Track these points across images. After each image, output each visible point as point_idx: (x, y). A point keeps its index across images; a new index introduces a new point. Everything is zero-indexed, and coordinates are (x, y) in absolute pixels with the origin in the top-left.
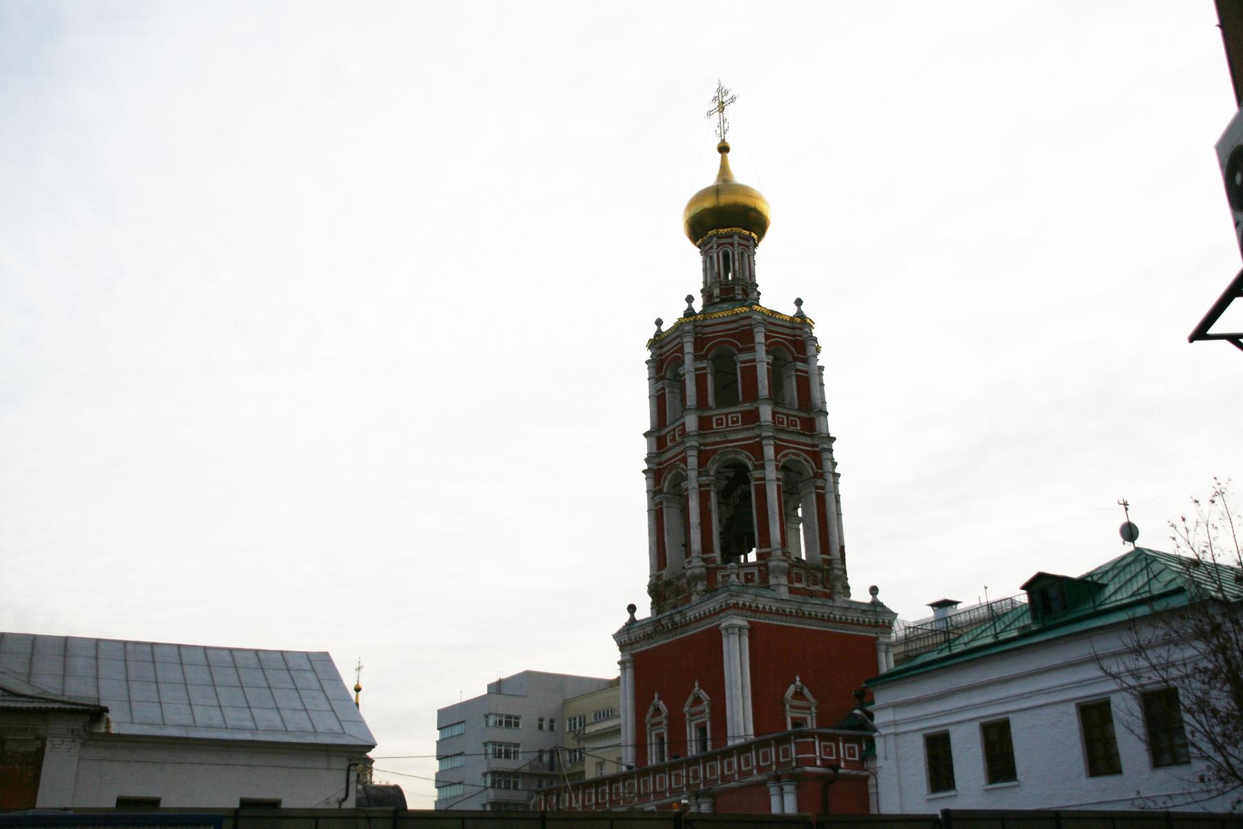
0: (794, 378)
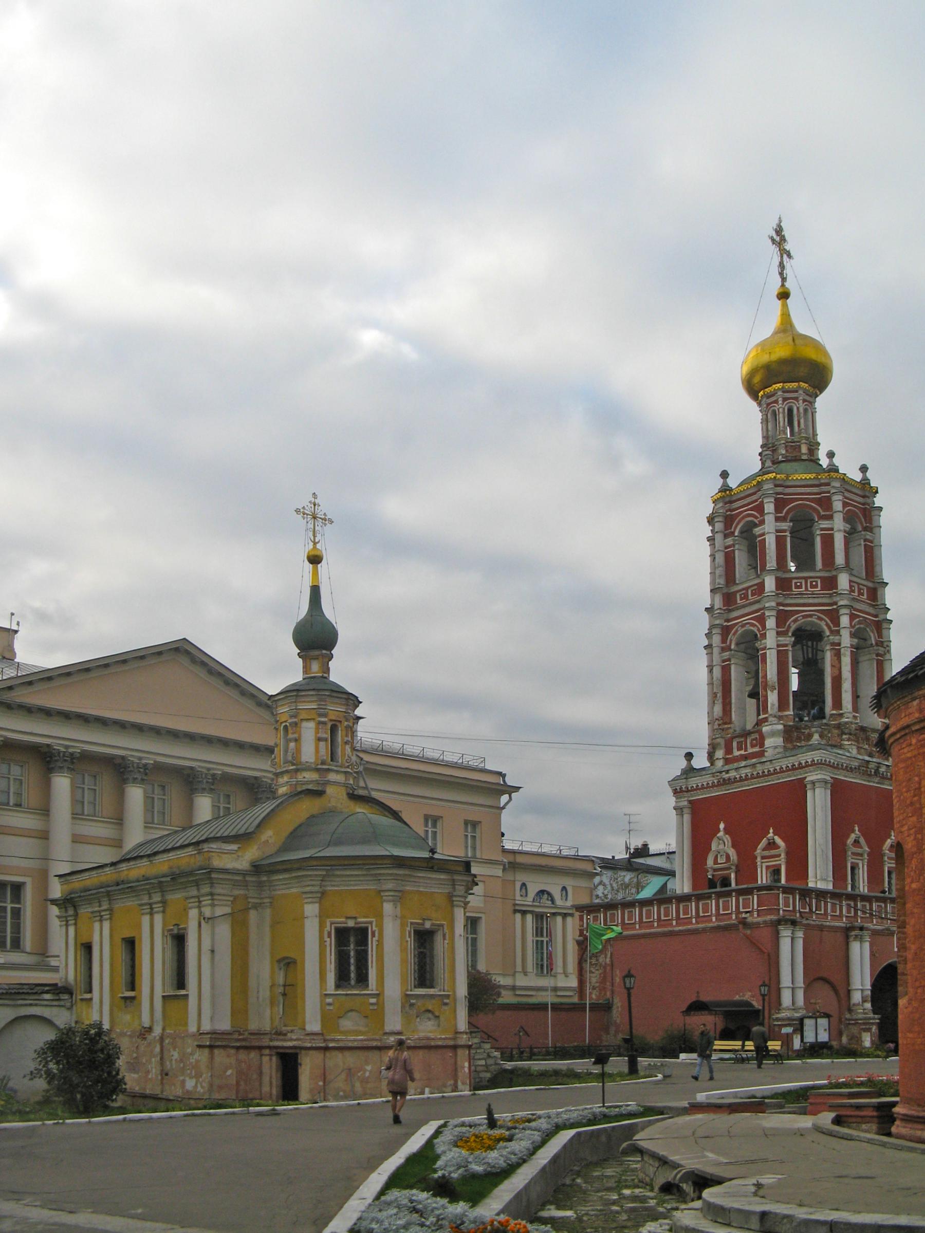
0: (818, 540)
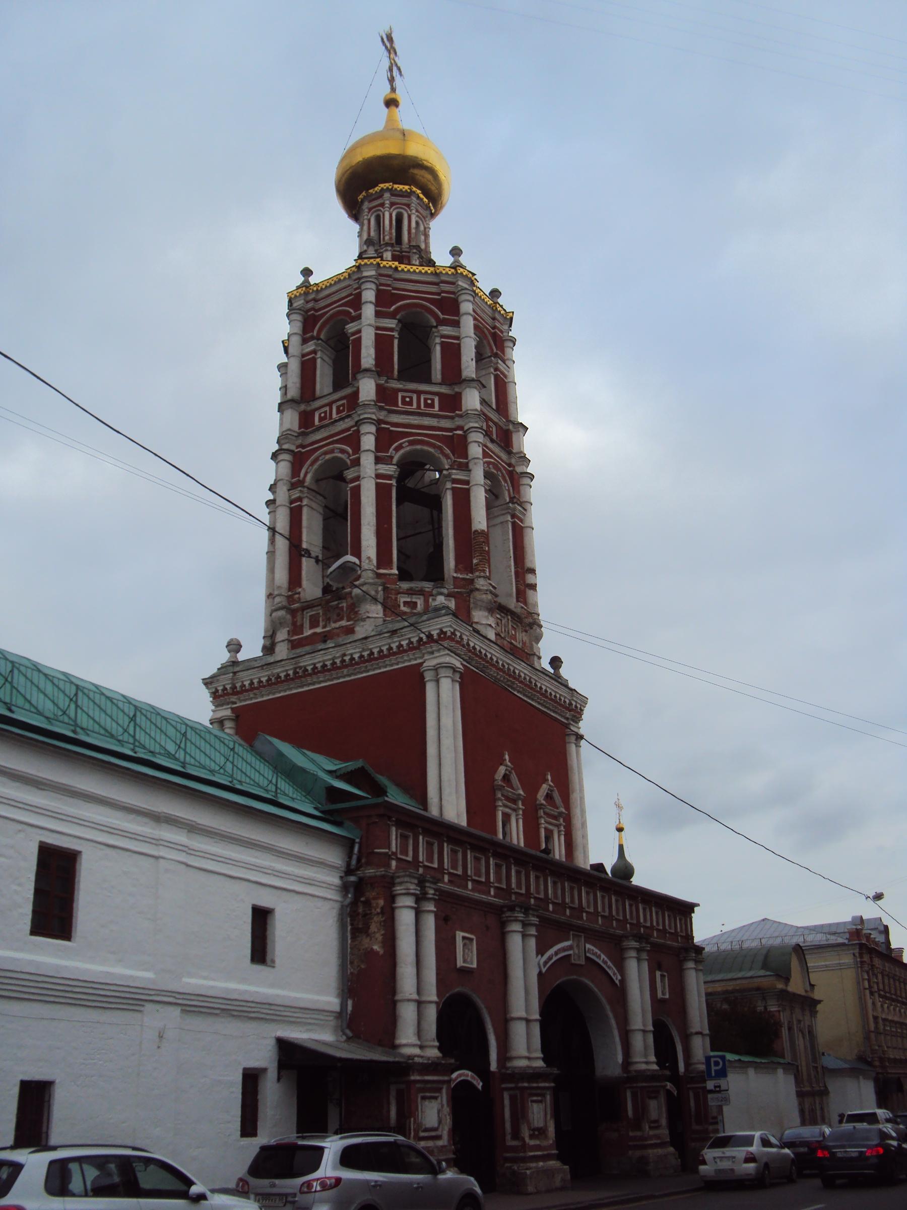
0: (438, 348)
